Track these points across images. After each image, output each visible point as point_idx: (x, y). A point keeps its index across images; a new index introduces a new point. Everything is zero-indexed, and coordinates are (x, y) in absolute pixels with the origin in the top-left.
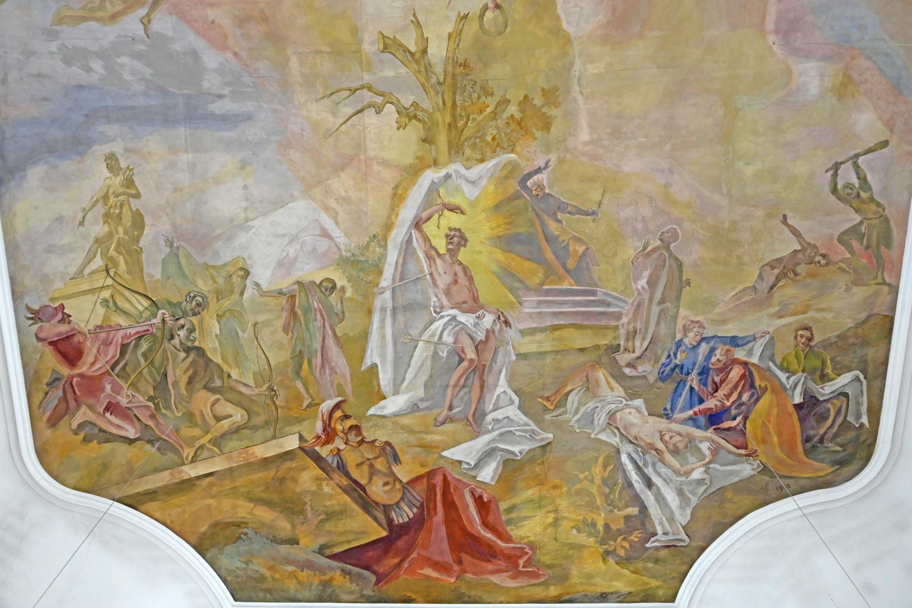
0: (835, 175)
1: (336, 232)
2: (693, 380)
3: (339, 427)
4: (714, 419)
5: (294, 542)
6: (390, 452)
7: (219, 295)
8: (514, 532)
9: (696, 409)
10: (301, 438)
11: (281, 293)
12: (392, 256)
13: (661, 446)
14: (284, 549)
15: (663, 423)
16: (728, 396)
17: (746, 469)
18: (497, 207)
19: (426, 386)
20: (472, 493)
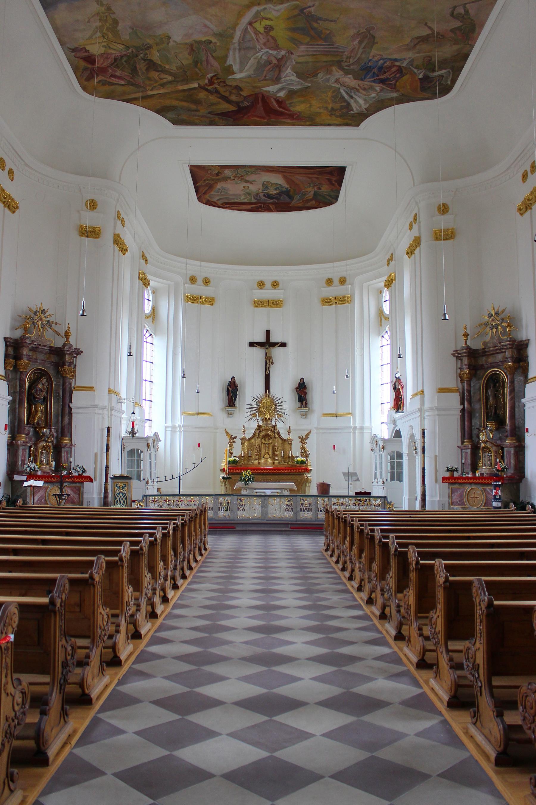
0: (454, 9)
1: (212, 26)
2: (376, 70)
3: (216, 81)
4: (382, 81)
5: (197, 111)
6: (238, 88)
7: (157, 44)
8: (292, 109)
9: (375, 78)
10: (198, 84)
11: (186, 44)
12: (238, 33)
13: (358, 88)
14: (193, 113)
15: (360, 82)
16: (390, 75)
17: (395, 95)
18: (288, 19)
19: (254, 71)
20: (275, 99)
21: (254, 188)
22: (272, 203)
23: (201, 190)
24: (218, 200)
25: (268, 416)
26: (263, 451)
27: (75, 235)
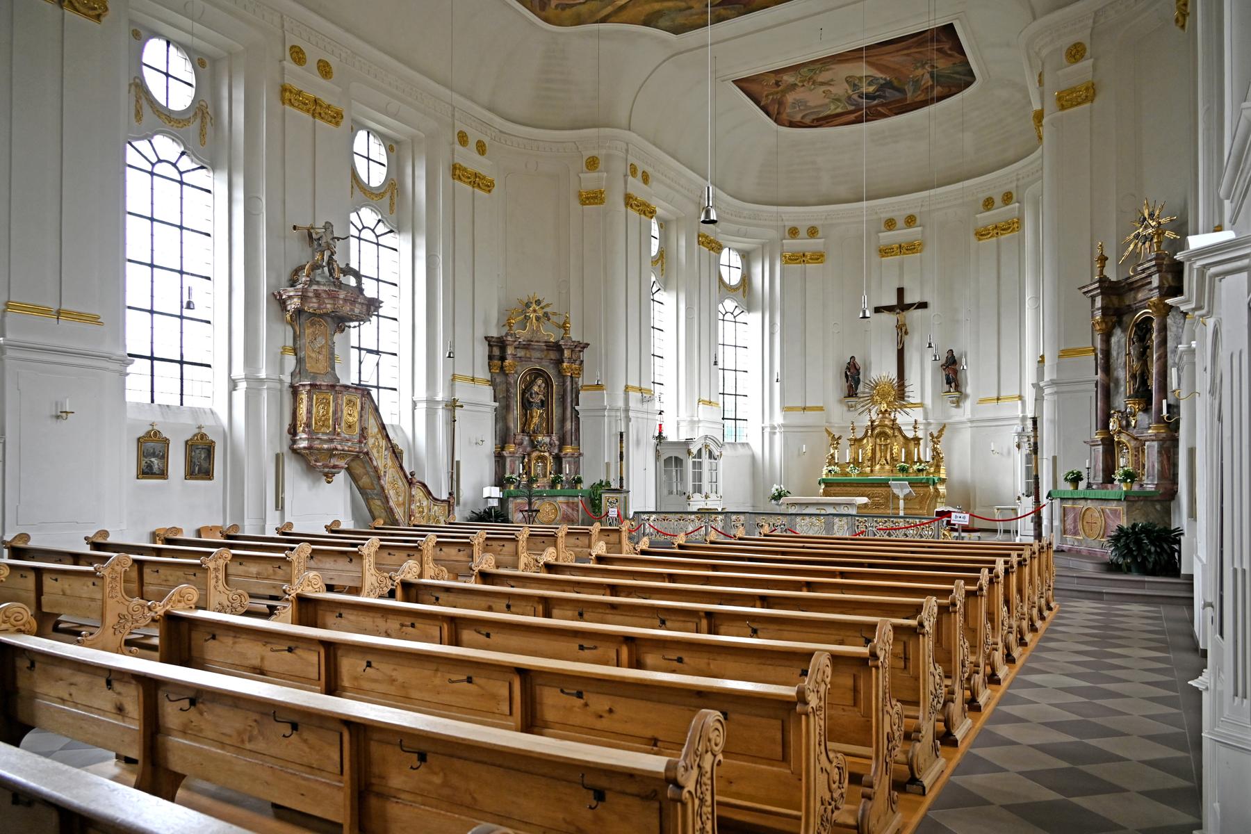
21: (841, 89)
22: (882, 105)
23: (770, 109)
24: (803, 117)
25: (884, 407)
26: (878, 455)
27: (575, 204)
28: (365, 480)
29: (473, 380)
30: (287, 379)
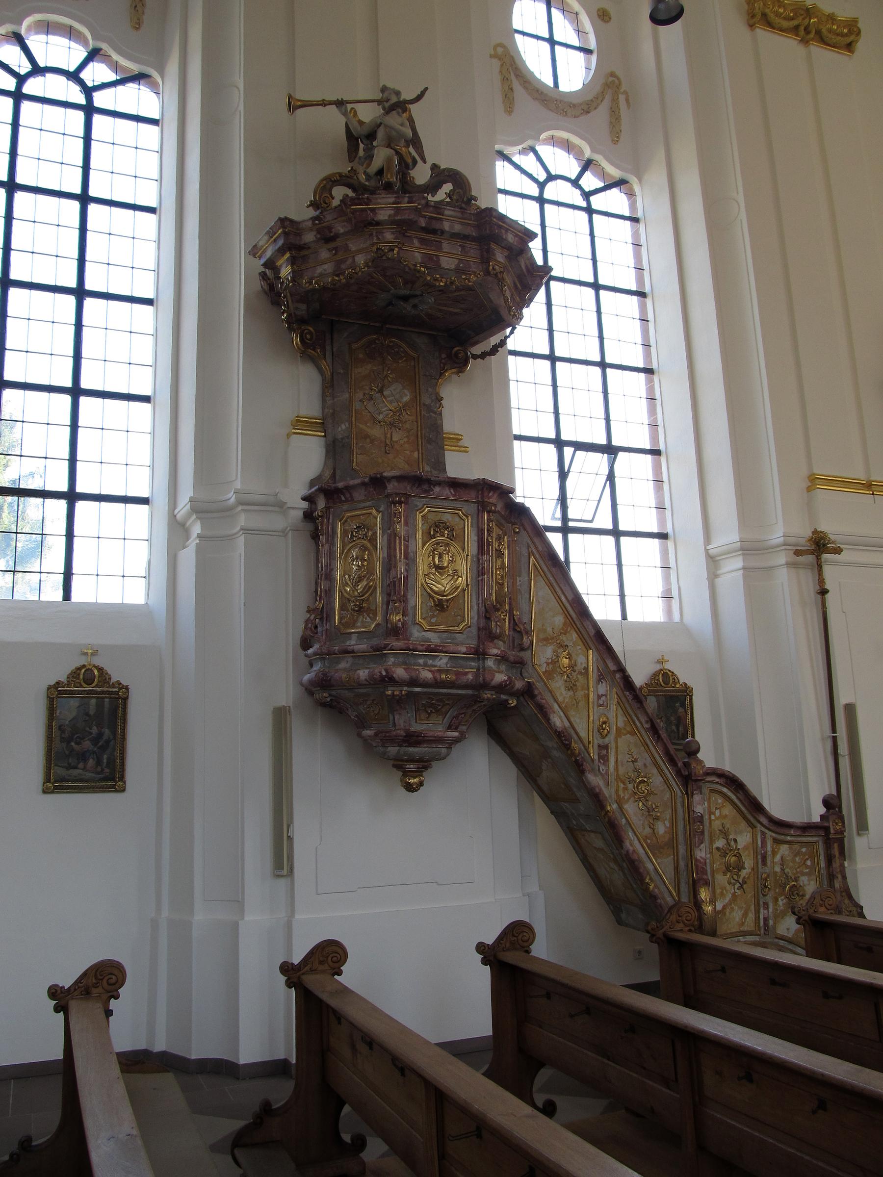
28: (547, 774)
29: (869, 486)
30: (294, 495)
